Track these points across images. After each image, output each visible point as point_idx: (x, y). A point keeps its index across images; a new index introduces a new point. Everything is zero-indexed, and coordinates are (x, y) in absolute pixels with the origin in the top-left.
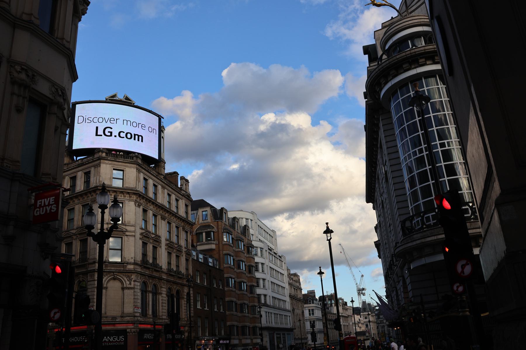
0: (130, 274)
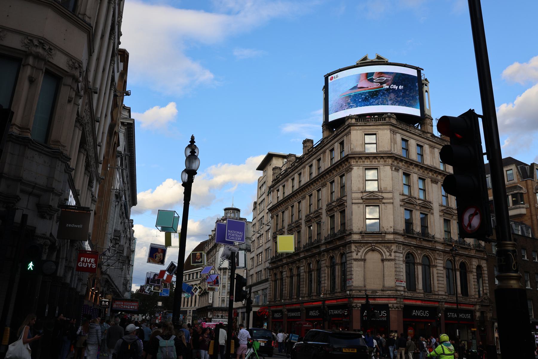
0: (389, 245)
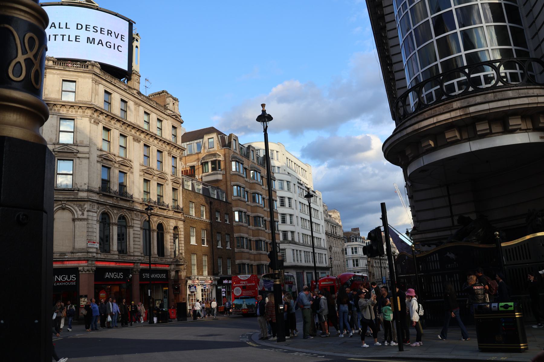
0: (82, 203)
